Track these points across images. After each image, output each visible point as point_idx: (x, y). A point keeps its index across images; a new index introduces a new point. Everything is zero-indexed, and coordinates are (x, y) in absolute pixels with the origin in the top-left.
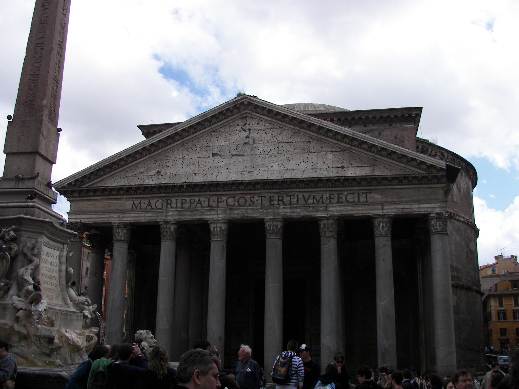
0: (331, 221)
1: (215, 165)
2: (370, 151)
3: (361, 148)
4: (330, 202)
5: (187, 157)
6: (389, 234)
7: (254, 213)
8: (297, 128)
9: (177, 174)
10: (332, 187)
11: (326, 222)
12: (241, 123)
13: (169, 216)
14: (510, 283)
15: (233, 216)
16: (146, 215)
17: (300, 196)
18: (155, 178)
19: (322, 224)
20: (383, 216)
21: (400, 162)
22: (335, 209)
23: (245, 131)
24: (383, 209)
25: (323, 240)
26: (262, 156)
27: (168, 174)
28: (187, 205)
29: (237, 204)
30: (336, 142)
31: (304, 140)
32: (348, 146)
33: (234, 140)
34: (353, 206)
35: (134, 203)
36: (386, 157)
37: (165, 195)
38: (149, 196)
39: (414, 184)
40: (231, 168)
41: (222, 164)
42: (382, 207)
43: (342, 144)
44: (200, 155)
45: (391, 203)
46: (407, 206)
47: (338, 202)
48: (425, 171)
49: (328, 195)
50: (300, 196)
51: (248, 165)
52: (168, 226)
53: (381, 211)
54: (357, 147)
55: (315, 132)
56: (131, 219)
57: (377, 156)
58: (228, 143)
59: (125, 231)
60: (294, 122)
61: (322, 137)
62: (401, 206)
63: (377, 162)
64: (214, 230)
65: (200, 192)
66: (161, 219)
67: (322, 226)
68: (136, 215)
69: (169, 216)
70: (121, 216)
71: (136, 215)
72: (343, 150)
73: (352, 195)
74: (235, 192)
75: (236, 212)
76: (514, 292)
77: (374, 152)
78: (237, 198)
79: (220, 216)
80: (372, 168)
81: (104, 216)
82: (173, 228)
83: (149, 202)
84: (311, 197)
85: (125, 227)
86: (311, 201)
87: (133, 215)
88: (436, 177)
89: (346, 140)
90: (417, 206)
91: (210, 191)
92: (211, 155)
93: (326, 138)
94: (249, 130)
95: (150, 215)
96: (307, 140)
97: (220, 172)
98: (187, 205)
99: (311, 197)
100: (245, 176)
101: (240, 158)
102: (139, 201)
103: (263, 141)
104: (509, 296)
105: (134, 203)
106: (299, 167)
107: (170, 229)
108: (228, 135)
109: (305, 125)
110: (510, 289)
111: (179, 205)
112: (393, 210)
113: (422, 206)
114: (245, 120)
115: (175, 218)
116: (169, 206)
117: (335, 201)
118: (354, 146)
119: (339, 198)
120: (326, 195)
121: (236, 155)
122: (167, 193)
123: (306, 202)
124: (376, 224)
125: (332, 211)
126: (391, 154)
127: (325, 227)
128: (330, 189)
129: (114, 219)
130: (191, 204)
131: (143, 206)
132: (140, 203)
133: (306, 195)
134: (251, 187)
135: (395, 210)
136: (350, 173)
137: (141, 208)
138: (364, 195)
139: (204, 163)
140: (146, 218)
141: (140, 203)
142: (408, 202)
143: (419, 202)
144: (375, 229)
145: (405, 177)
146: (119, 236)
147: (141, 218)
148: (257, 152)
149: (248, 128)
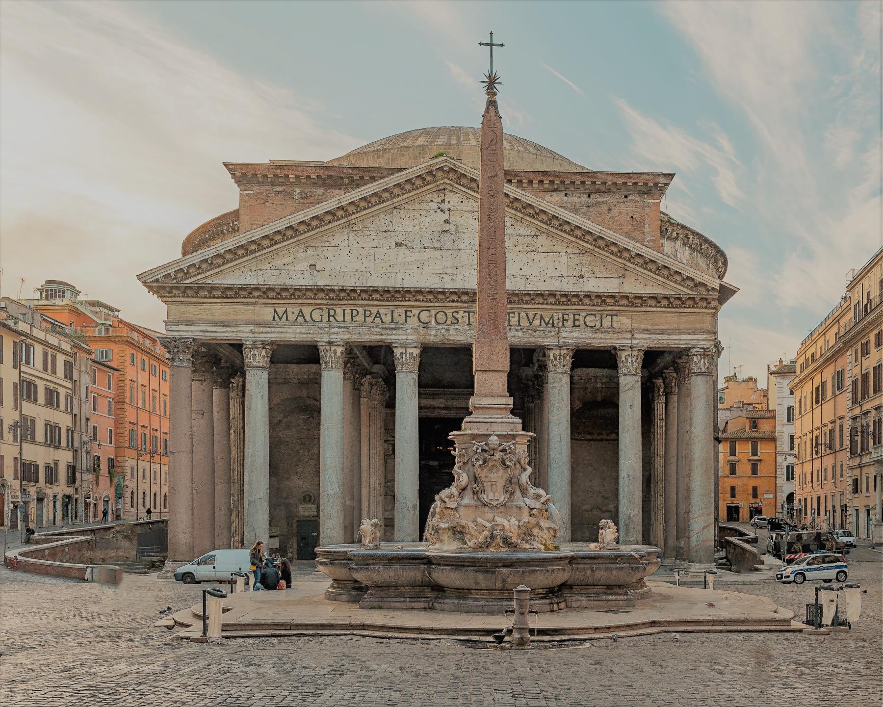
0: (563, 352)
1: (400, 260)
2: (620, 257)
3: (608, 251)
4: (563, 325)
5: (355, 245)
6: (639, 371)
7: (459, 335)
8: (519, 214)
9: (343, 270)
10: (567, 304)
11: (557, 352)
12: (438, 200)
13: (334, 333)
14: (748, 421)
15: (427, 337)
16: (298, 330)
17: (523, 314)
18: (307, 273)
19: (551, 353)
20: (632, 348)
21: (659, 274)
22: (569, 335)
23: (442, 211)
24: (632, 339)
25: (551, 376)
26: (468, 252)
27: (328, 270)
28: (360, 319)
29: (433, 320)
30: (574, 239)
31: (528, 233)
32: (591, 247)
33: (427, 225)
34: (595, 332)
35: (275, 311)
36: (642, 267)
37: (325, 302)
38: (300, 301)
39: (676, 307)
40: (425, 266)
41: (408, 259)
42: (630, 336)
43: (581, 243)
44: (375, 243)
45: (643, 331)
46: (663, 337)
47: (574, 325)
48: (691, 289)
49: (560, 316)
50: (523, 314)
51: (449, 264)
52: (333, 348)
53: (630, 342)
54: (603, 249)
55: (546, 223)
56: (273, 336)
57: (629, 264)
58: (417, 227)
59: (264, 353)
60: (516, 204)
61: (555, 231)
62: (657, 336)
63: (627, 272)
64: (402, 357)
65: (380, 300)
66: (321, 337)
67: (552, 357)
68: (281, 330)
69: (334, 333)
70: (256, 330)
71: (281, 330)
72: (582, 253)
73: (593, 318)
74: (432, 304)
75: (433, 332)
76: (753, 435)
77: (625, 259)
78: (433, 312)
79: (409, 337)
80: (621, 280)
81: (228, 329)
82: (339, 350)
83: (301, 311)
84: (538, 317)
85: (264, 348)
86: (537, 322)
87: (277, 330)
88: (706, 299)
89: (588, 237)
90: (677, 337)
91: (395, 300)
92: (393, 246)
93: (560, 233)
94: (449, 210)
95: (303, 330)
96: (533, 233)
97: (408, 271)
98: (360, 319)
99: (538, 317)
100: (445, 280)
101: (437, 253)
102: (284, 309)
103: (470, 230)
104: (747, 439)
105: (275, 311)
106: (521, 272)
107: (335, 354)
108: (417, 215)
109: (531, 212)
110: (748, 430)
111: (348, 318)
112: (646, 341)
113: (683, 337)
114: (443, 195)
115: (342, 336)
116: (332, 319)
117: (569, 324)
118: (599, 247)
119: (575, 320)
120: (558, 316)
121: (431, 248)
122: (329, 299)
123: (531, 324)
124: (623, 359)
125: (564, 338)
126: (648, 263)
127: (555, 359)
128: (564, 307)
129: (245, 335)
130: (365, 317)
131: (292, 317)
132: (286, 311)
133: (531, 316)
134: (455, 297)
135: (648, 341)
136: (591, 286)
137: (287, 320)
138: (609, 317)
139: (383, 257)
140: (298, 336)
141: (286, 311)
142: (664, 331)
143: (680, 332)
144: (620, 365)
145: (666, 298)
146: (254, 360)
147: (288, 335)
148: (461, 246)
149: (447, 208)
